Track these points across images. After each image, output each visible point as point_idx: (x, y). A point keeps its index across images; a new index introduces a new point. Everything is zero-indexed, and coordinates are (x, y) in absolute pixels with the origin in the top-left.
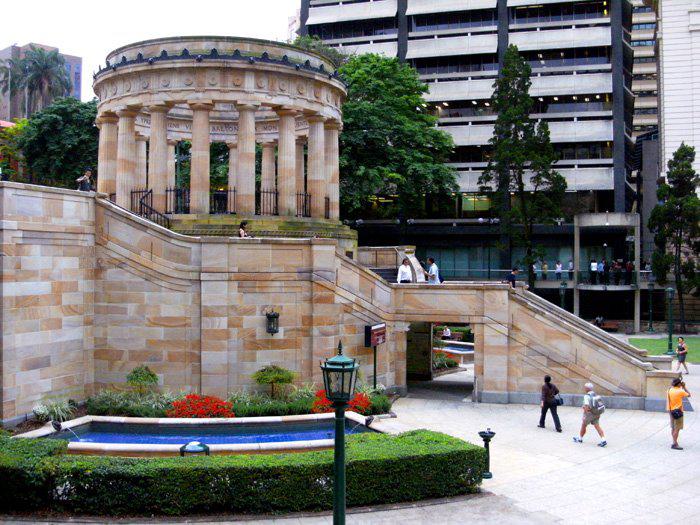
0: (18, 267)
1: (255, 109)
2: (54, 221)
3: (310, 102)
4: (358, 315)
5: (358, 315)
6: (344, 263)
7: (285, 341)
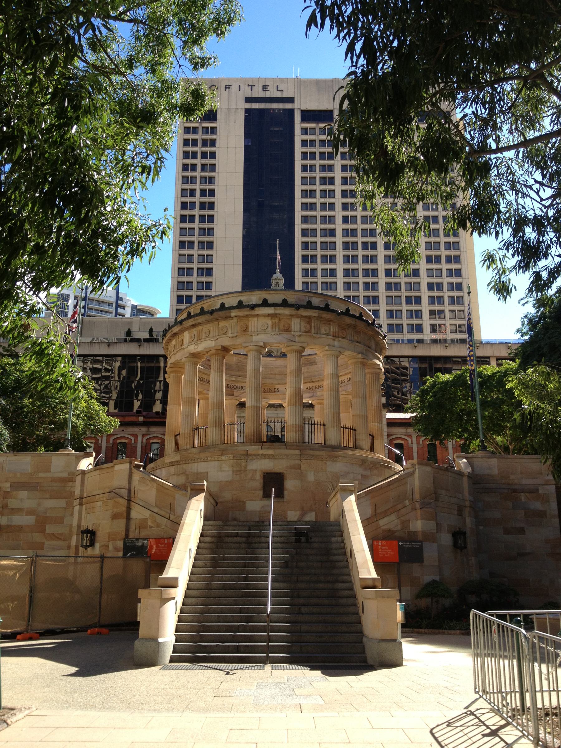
0: (5, 506)
2: (41, 475)
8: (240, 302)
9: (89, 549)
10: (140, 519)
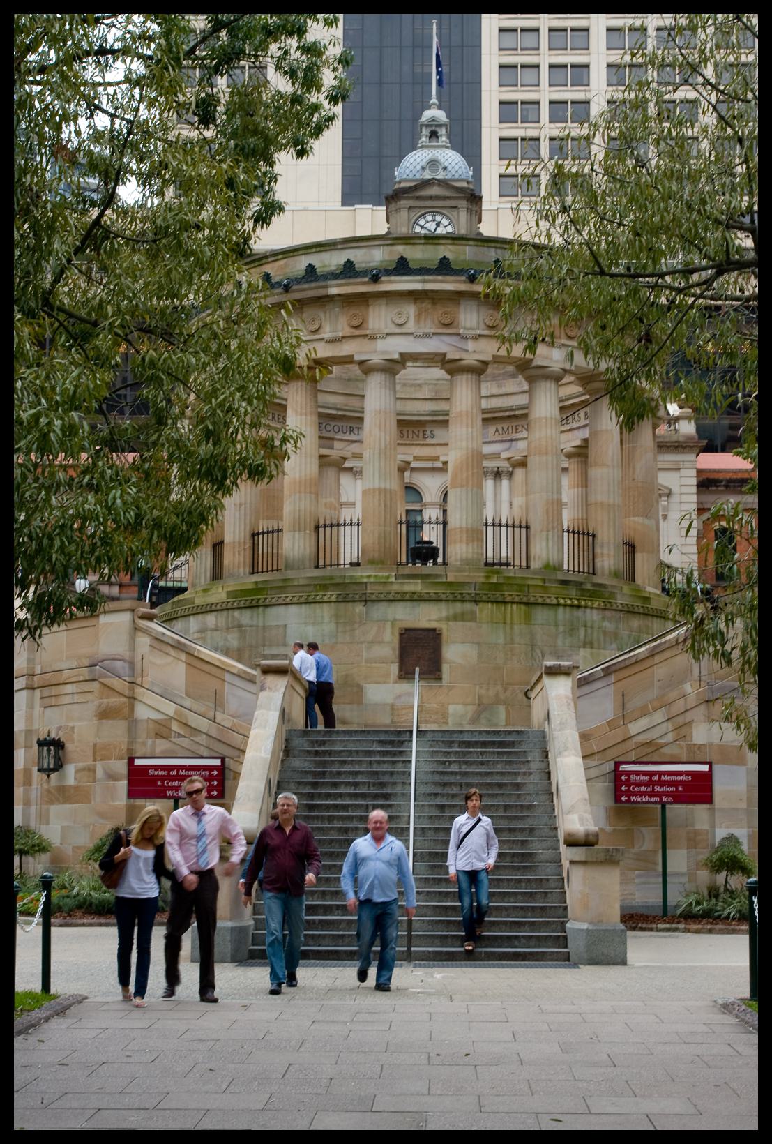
1: (391, 367)
3: (332, 341)
4: (185, 742)
5: (185, 742)
6: (156, 644)
7: (76, 788)
8: (349, 264)
9: (53, 776)
10: (155, 721)
